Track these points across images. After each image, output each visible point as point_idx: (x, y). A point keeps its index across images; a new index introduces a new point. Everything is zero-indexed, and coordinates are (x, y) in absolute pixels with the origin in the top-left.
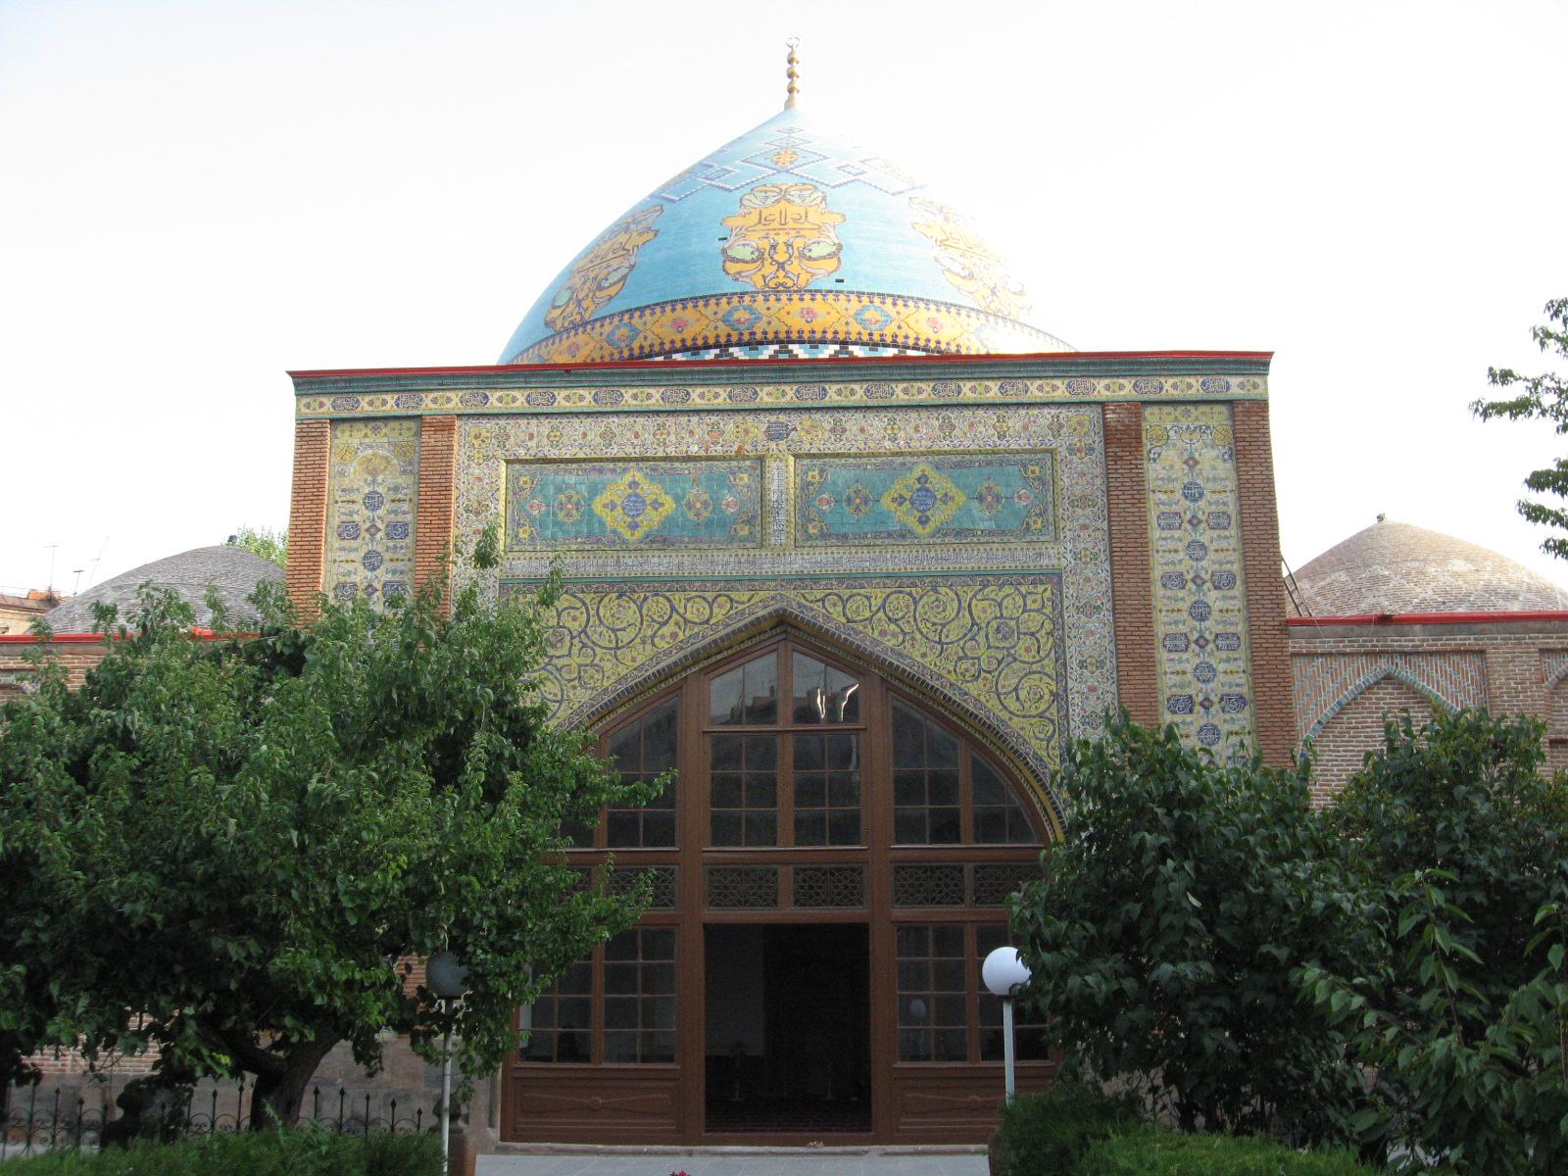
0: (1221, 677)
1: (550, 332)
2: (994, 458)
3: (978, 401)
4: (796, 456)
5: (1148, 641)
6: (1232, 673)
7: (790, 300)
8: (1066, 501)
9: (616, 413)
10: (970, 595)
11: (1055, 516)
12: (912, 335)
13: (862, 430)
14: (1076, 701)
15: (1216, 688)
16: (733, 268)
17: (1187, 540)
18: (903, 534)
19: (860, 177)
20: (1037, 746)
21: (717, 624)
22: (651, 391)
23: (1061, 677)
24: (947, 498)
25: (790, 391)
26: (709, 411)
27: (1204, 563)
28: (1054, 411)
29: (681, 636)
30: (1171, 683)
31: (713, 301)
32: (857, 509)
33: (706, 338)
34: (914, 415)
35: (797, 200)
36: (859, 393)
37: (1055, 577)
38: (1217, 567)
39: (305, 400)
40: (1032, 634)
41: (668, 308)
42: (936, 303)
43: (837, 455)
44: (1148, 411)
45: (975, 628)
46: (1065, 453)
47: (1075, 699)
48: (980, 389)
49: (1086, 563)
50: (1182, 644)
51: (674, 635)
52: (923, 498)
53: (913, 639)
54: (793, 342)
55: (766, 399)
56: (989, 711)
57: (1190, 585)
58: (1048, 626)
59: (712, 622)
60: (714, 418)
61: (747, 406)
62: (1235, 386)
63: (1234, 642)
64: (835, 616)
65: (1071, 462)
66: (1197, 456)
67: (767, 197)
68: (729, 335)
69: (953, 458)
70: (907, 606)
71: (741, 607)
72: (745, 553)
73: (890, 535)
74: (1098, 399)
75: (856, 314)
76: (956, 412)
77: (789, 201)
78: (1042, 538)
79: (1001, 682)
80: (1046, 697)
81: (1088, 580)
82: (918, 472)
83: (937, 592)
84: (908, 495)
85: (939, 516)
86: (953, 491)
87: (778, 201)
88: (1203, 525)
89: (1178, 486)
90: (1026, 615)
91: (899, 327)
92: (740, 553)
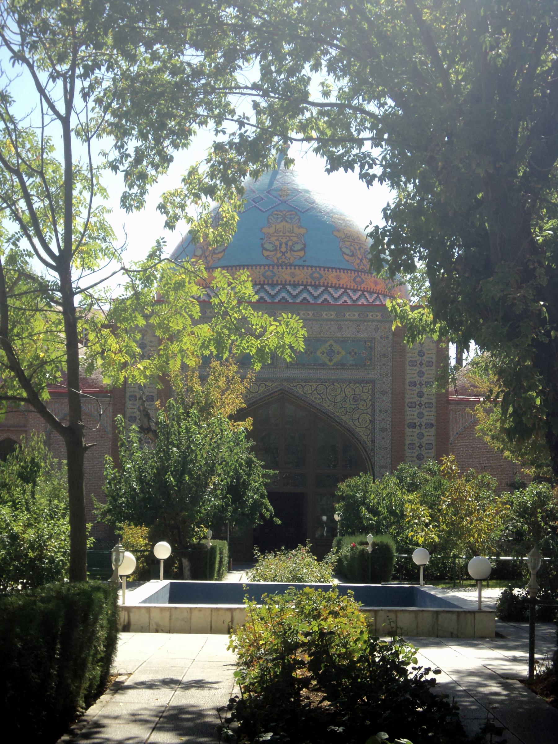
0: (426, 417)
6: (430, 416)
12: (330, 283)
13: (311, 328)
15: (424, 421)
16: (266, 253)
17: (418, 370)
18: (324, 365)
20: (364, 438)
23: (373, 415)
24: (338, 353)
27: (423, 378)
31: (258, 267)
34: (329, 323)
35: (289, 220)
37: (373, 382)
46: (379, 338)
50: (414, 405)
52: (331, 353)
57: (418, 386)
58: (370, 398)
63: (431, 405)
67: (277, 218)
77: (287, 221)
81: (384, 383)
82: (329, 343)
84: (326, 351)
87: (282, 221)
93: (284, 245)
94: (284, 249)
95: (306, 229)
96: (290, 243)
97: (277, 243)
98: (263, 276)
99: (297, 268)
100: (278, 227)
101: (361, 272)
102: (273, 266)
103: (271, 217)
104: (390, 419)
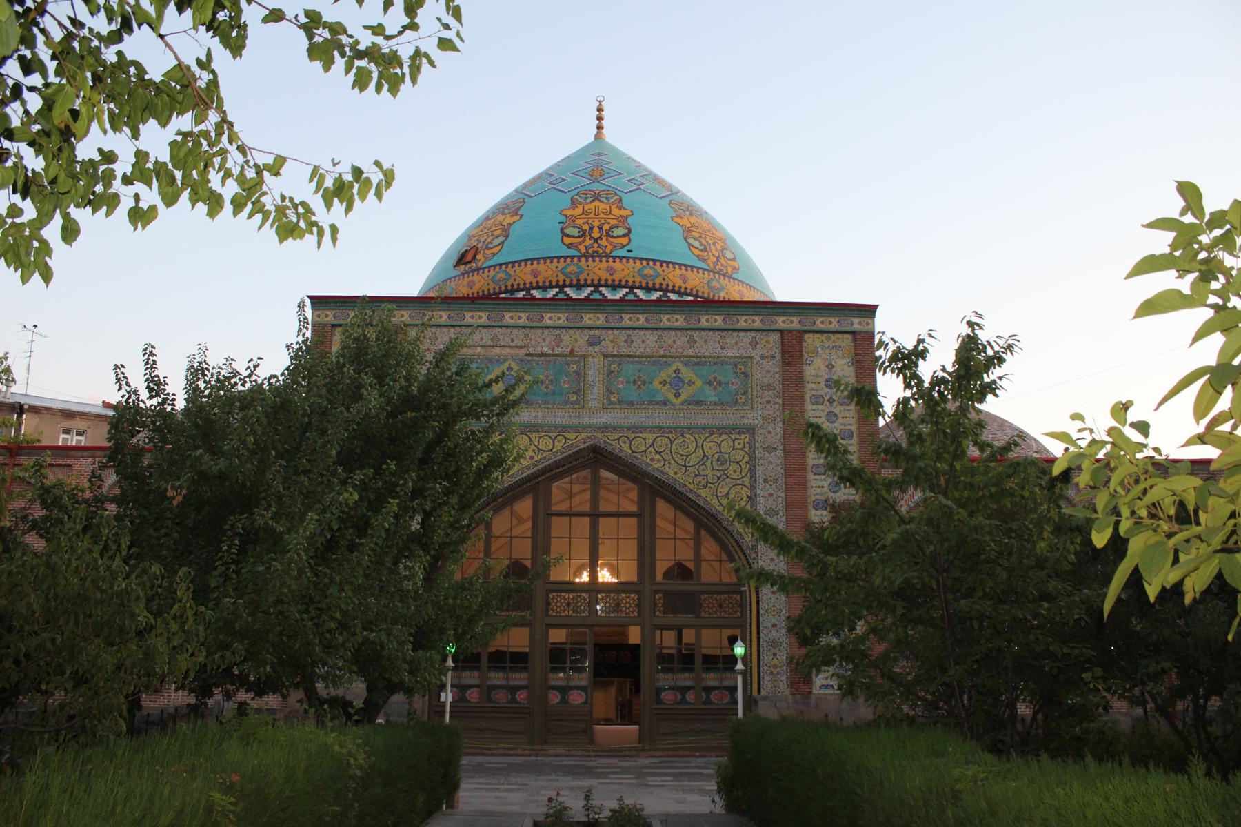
1: (456, 273)
2: (718, 361)
3: (710, 327)
4: (605, 356)
5: (804, 470)
7: (601, 261)
8: (759, 387)
9: (501, 327)
10: (703, 439)
11: (752, 395)
13: (643, 342)
14: (761, 501)
18: (665, 403)
19: (642, 187)
21: (557, 452)
22: (522, 315)
23: (753, 488)
24: (691, 383)
25: (602, 317)
26: (555, 328)
28: (753, 334)
29: (536, 458)
30: (815, 492)
31: (555, 260)
32: (639, 388)
33: (551, 282)
35: (605, 201)
36: (641, 320)
37: (751, 431)
38: (842, 427)
39: (317, 313)
40: (738, 463)
41: (529, 263)
42: (685, 265)
43: (628, 356)
44: (807, 335)
45: (705, 458)
46: (759, 359)
47: (761, 500)
48: (711, 320)
49: (769, 423)
51: (532, 458)
52: (677, 382)
53: (669, 463)
54: (602, 286)
55: (588, 322)
56: (712, 506)
58: (747, 458)
59: (554, 450)
60: (558, 332)
61: (576, 326)
62: (857, 324)
64: (625, 449)
65: (762, 364)
66: (833, 363)
67: (587, 198)
68: (564, 281)
69: (694, 359)
70: (667, 445)
71: (571, 442)
72: (574, 410)
73: (658, 403)
74: (781, 329)
75: (639, 271)
76: (697, 333)
77: (600, 201)
78: (745, 408)
79: (719, 490)
80: (745, 499)
81: (770, 432)
82: (674, 368)
83: (684, 437)
85: (686, 393)
86: (694, 378)
87: (594, 201)
88: (835, 403)
89: (822, 380)
90: (734, 452)
91: (664, 279)
92: (571, 411)
93: (596, 230)
94: (596, 234)
95: (632, 211)
96: (606, 227)
97: (586, 227)
98: (562, 271)
99: (618, 260)
100: (586, 207)
101: (720, 274)
102: (579, 257)
103: (577, 197)
104: (783, 495)
